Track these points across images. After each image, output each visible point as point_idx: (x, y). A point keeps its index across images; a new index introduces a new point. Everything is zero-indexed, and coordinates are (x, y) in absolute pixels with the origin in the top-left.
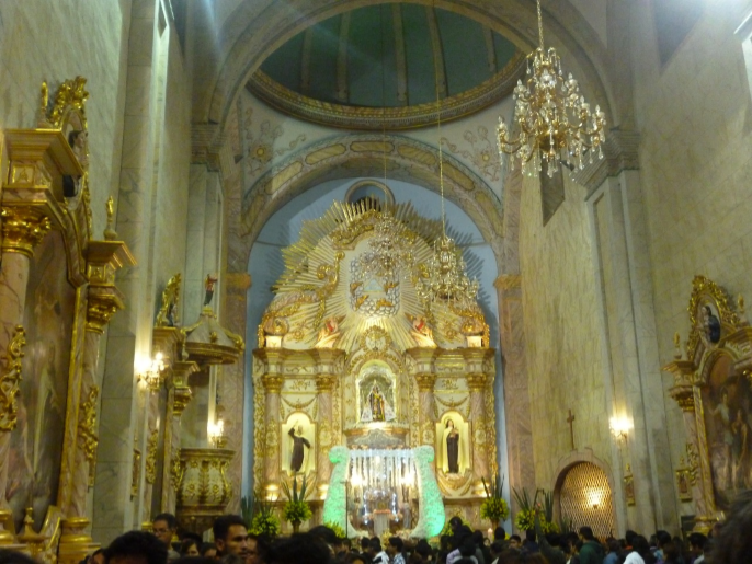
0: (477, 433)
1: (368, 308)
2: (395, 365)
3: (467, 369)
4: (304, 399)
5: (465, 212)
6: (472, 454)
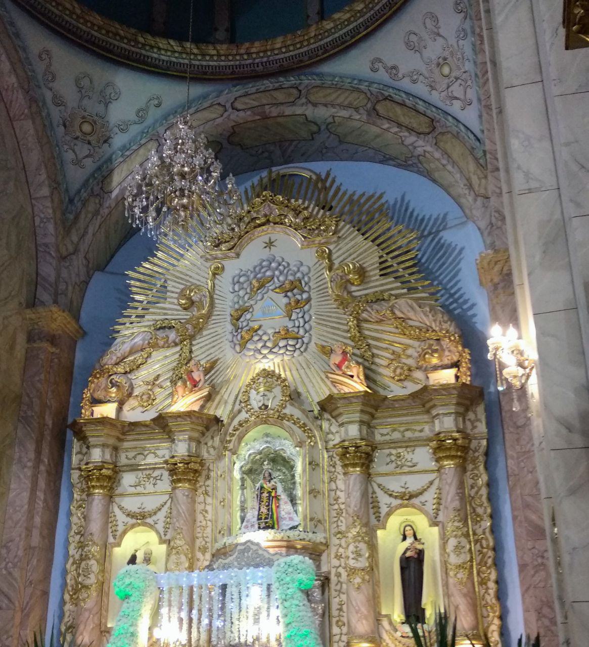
0: (452, 542)
1: (260, 345)
2: (299, 431)
4: (150, 504)
5: (434, 181)
6: (446, 585)
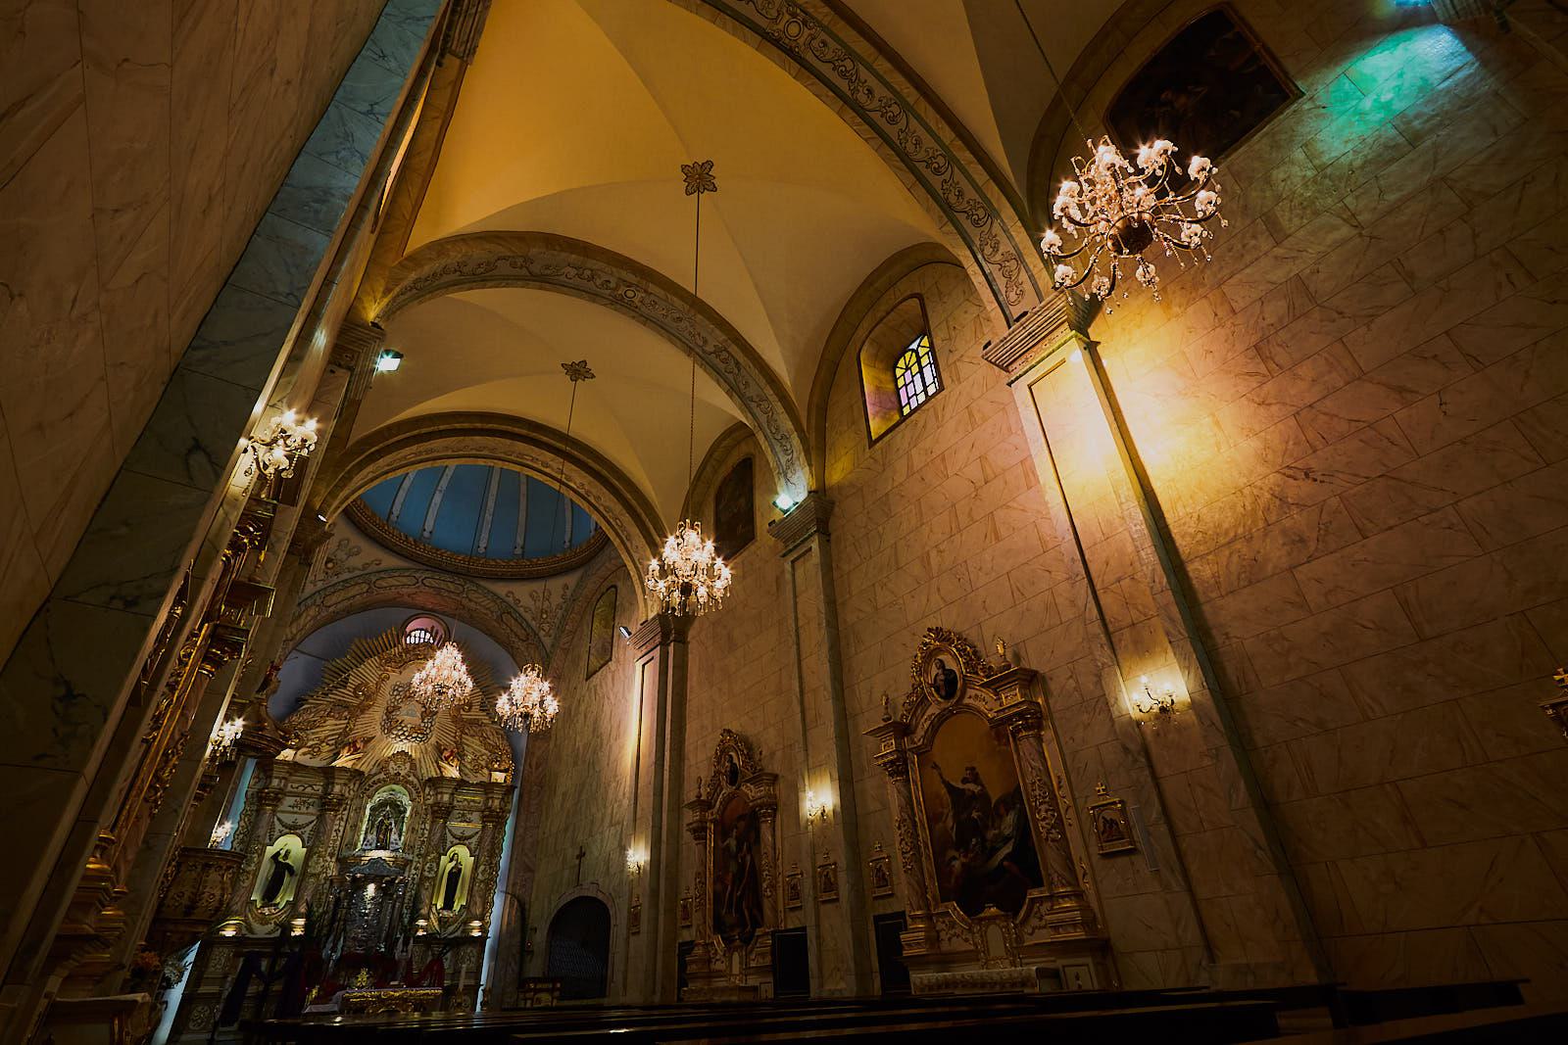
1: (400, 733)
3: (486, 804)
4: (302, 820)
6: (471, 890)
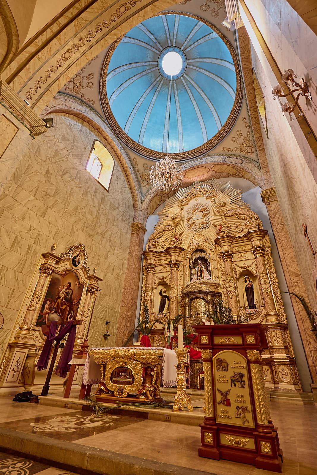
5: (245, 178)
